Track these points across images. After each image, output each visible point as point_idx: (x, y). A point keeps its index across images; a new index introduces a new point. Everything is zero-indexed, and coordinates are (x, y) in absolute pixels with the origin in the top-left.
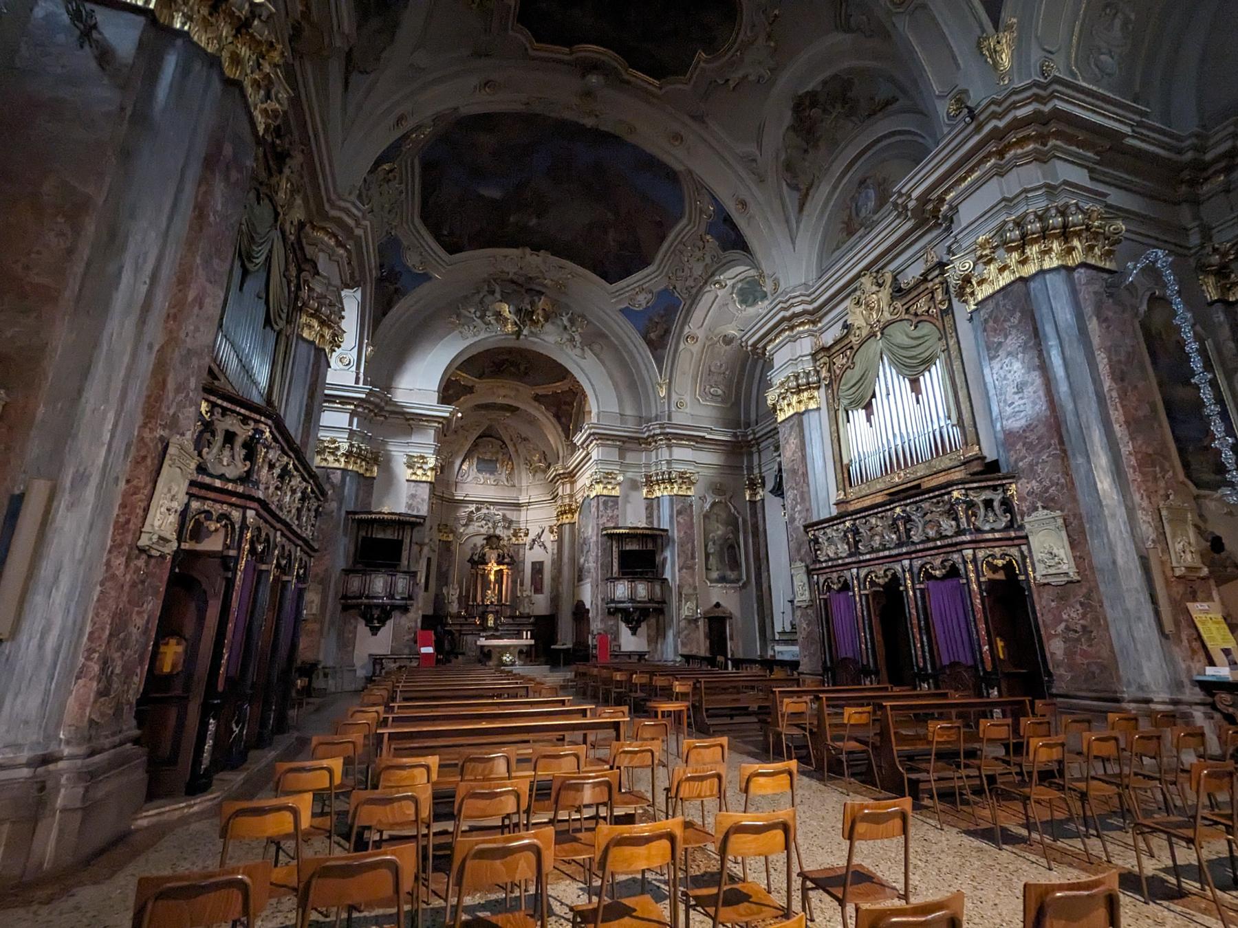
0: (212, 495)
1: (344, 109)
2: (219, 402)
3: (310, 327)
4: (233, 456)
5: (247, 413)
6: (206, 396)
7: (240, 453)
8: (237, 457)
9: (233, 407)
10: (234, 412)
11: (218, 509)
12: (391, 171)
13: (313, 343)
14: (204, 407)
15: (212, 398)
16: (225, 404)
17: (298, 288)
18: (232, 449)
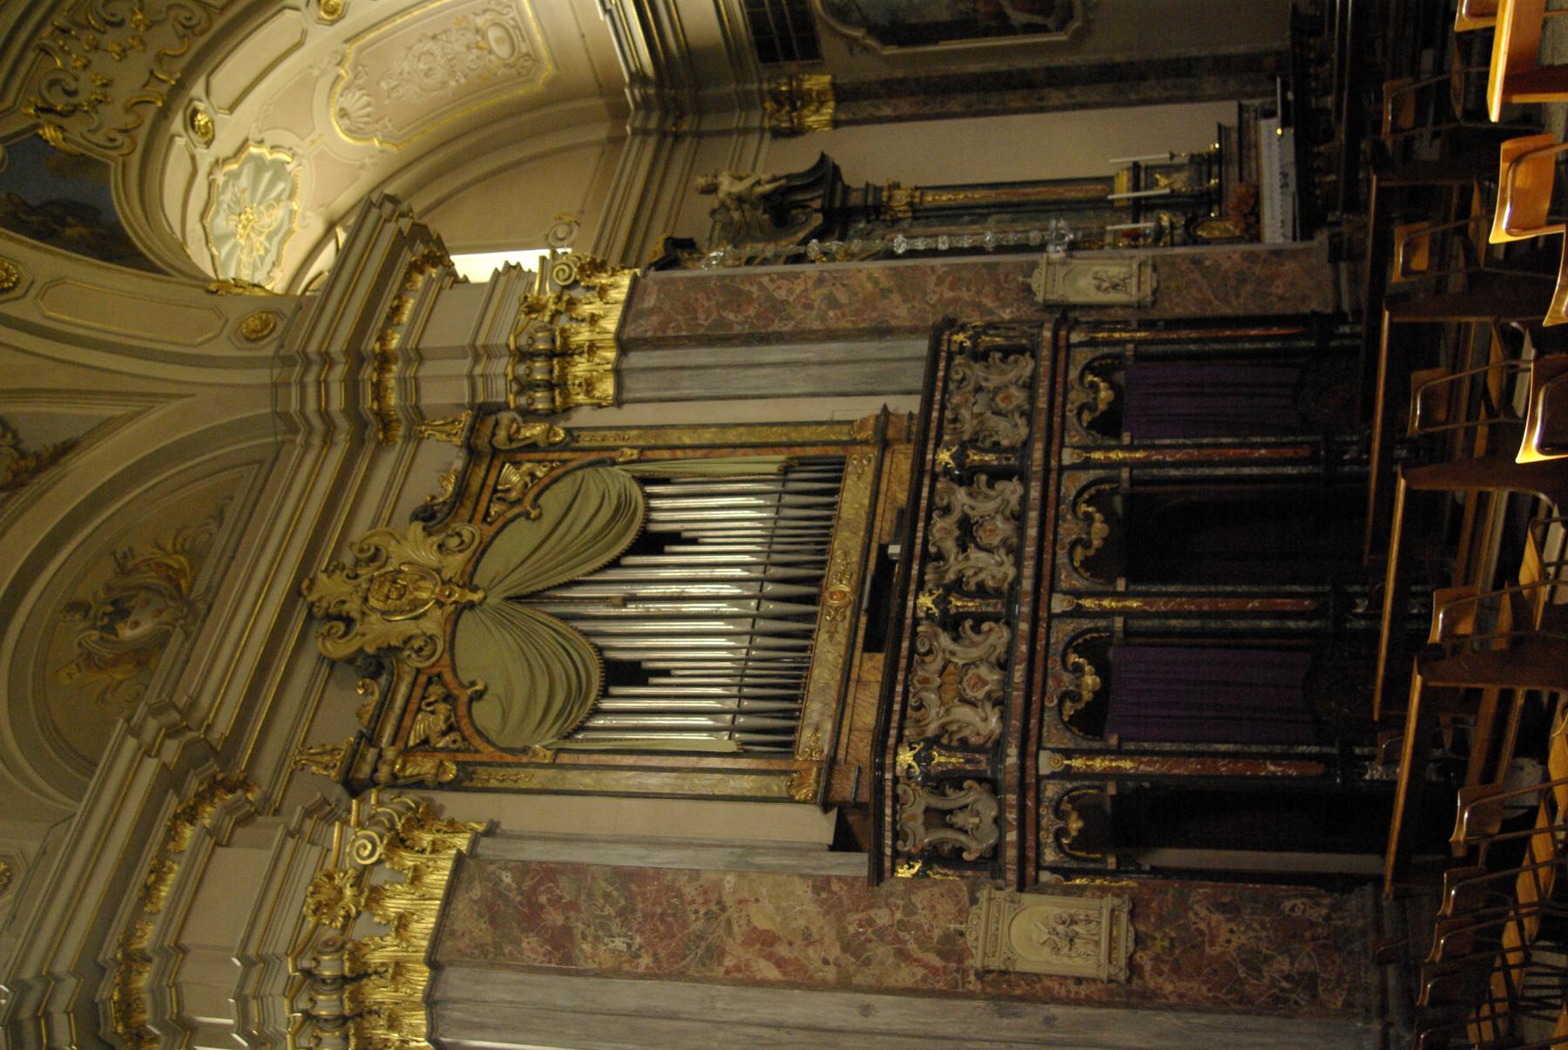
0: (1031, 839)
1: (107, 426)
2: (888, 851)
3: (589, 386)
4: (963, 808)
5: (888, 802)
6: (887, 875)
7: (954, 798)
8: (962, 802)
9: (888, 827)
10: (894, 822)
11: (1047, 817)
12: (49, 110)
13: (618, 372)
14: (904, 872)
15: (888, 864)
16: (888, 842)
17: (532, 447)
18: (951, 812)
